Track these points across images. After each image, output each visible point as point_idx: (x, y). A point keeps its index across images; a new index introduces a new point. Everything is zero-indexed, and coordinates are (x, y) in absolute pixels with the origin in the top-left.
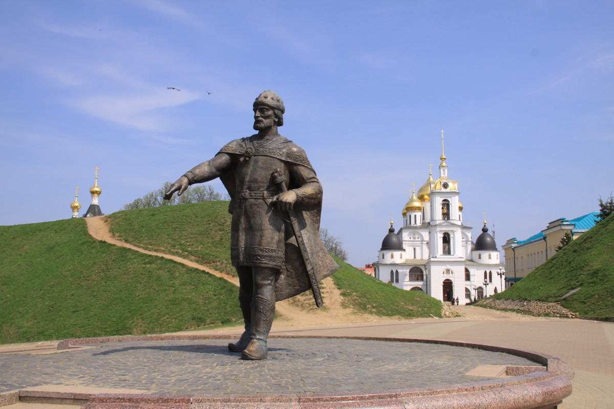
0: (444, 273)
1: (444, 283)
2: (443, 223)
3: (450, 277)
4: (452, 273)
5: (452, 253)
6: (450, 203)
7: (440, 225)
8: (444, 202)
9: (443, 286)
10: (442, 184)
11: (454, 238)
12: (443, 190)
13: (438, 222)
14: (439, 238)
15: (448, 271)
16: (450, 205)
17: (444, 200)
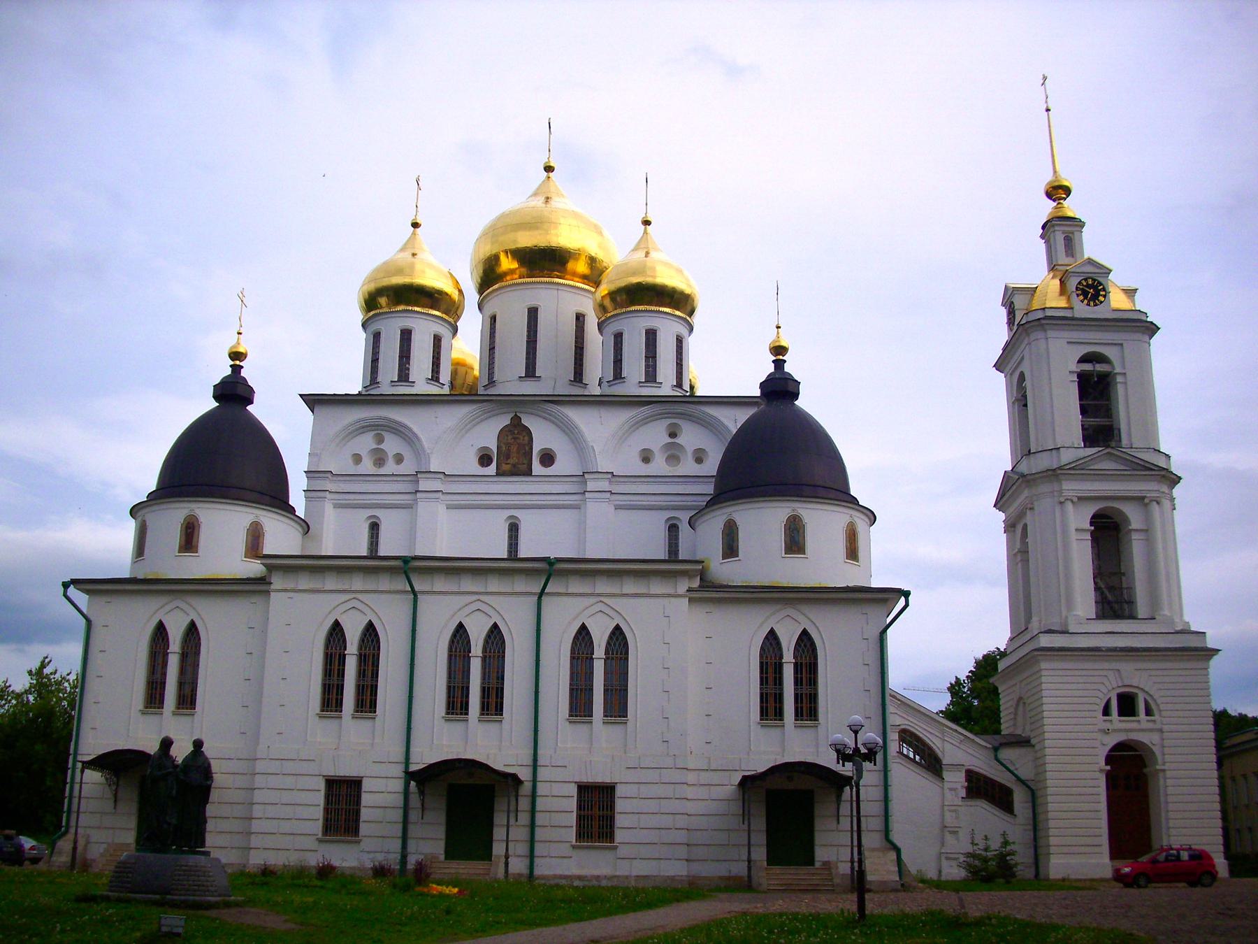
0: (1106, 712)
1: (1109, 759)
2: (1093, 459)
3: (1136, 729)
4: (1149, 712)
5: (1142, 609)
6: (1118, 370)
7: (1077, 470)
8: (1087, 367)
9: (1109, 776)
10: (1073, 283)
11: (1147, 531)
12: (1082, 309)
13: (1066, 457)
14: (1074, 536)
15: (1127, 704)
16: (1119, 379)
17: (1083, 360)
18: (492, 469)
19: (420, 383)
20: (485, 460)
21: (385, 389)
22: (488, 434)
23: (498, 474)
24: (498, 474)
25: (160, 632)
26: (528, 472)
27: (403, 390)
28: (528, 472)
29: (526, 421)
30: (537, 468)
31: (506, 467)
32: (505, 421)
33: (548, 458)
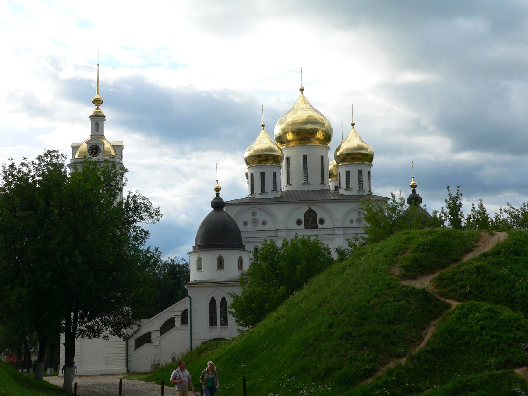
18: (303, 226)
19: (270, 195)
20: (299, 222)
21: (258, 196)
22: (301, 213)
23: (306, 228)
24: (306, 228)
25: (213, 301)
26: (316, 227)
27: (264, 197)
28: (316, 227)
29: (314, 208)
30: (319, 226)
31: (308, 226)
32: (306, 209)
33: (322, 221)
